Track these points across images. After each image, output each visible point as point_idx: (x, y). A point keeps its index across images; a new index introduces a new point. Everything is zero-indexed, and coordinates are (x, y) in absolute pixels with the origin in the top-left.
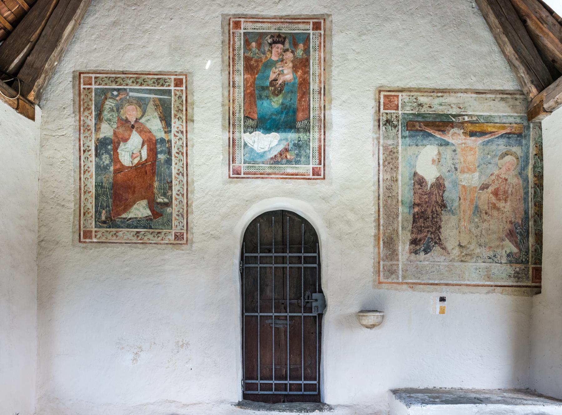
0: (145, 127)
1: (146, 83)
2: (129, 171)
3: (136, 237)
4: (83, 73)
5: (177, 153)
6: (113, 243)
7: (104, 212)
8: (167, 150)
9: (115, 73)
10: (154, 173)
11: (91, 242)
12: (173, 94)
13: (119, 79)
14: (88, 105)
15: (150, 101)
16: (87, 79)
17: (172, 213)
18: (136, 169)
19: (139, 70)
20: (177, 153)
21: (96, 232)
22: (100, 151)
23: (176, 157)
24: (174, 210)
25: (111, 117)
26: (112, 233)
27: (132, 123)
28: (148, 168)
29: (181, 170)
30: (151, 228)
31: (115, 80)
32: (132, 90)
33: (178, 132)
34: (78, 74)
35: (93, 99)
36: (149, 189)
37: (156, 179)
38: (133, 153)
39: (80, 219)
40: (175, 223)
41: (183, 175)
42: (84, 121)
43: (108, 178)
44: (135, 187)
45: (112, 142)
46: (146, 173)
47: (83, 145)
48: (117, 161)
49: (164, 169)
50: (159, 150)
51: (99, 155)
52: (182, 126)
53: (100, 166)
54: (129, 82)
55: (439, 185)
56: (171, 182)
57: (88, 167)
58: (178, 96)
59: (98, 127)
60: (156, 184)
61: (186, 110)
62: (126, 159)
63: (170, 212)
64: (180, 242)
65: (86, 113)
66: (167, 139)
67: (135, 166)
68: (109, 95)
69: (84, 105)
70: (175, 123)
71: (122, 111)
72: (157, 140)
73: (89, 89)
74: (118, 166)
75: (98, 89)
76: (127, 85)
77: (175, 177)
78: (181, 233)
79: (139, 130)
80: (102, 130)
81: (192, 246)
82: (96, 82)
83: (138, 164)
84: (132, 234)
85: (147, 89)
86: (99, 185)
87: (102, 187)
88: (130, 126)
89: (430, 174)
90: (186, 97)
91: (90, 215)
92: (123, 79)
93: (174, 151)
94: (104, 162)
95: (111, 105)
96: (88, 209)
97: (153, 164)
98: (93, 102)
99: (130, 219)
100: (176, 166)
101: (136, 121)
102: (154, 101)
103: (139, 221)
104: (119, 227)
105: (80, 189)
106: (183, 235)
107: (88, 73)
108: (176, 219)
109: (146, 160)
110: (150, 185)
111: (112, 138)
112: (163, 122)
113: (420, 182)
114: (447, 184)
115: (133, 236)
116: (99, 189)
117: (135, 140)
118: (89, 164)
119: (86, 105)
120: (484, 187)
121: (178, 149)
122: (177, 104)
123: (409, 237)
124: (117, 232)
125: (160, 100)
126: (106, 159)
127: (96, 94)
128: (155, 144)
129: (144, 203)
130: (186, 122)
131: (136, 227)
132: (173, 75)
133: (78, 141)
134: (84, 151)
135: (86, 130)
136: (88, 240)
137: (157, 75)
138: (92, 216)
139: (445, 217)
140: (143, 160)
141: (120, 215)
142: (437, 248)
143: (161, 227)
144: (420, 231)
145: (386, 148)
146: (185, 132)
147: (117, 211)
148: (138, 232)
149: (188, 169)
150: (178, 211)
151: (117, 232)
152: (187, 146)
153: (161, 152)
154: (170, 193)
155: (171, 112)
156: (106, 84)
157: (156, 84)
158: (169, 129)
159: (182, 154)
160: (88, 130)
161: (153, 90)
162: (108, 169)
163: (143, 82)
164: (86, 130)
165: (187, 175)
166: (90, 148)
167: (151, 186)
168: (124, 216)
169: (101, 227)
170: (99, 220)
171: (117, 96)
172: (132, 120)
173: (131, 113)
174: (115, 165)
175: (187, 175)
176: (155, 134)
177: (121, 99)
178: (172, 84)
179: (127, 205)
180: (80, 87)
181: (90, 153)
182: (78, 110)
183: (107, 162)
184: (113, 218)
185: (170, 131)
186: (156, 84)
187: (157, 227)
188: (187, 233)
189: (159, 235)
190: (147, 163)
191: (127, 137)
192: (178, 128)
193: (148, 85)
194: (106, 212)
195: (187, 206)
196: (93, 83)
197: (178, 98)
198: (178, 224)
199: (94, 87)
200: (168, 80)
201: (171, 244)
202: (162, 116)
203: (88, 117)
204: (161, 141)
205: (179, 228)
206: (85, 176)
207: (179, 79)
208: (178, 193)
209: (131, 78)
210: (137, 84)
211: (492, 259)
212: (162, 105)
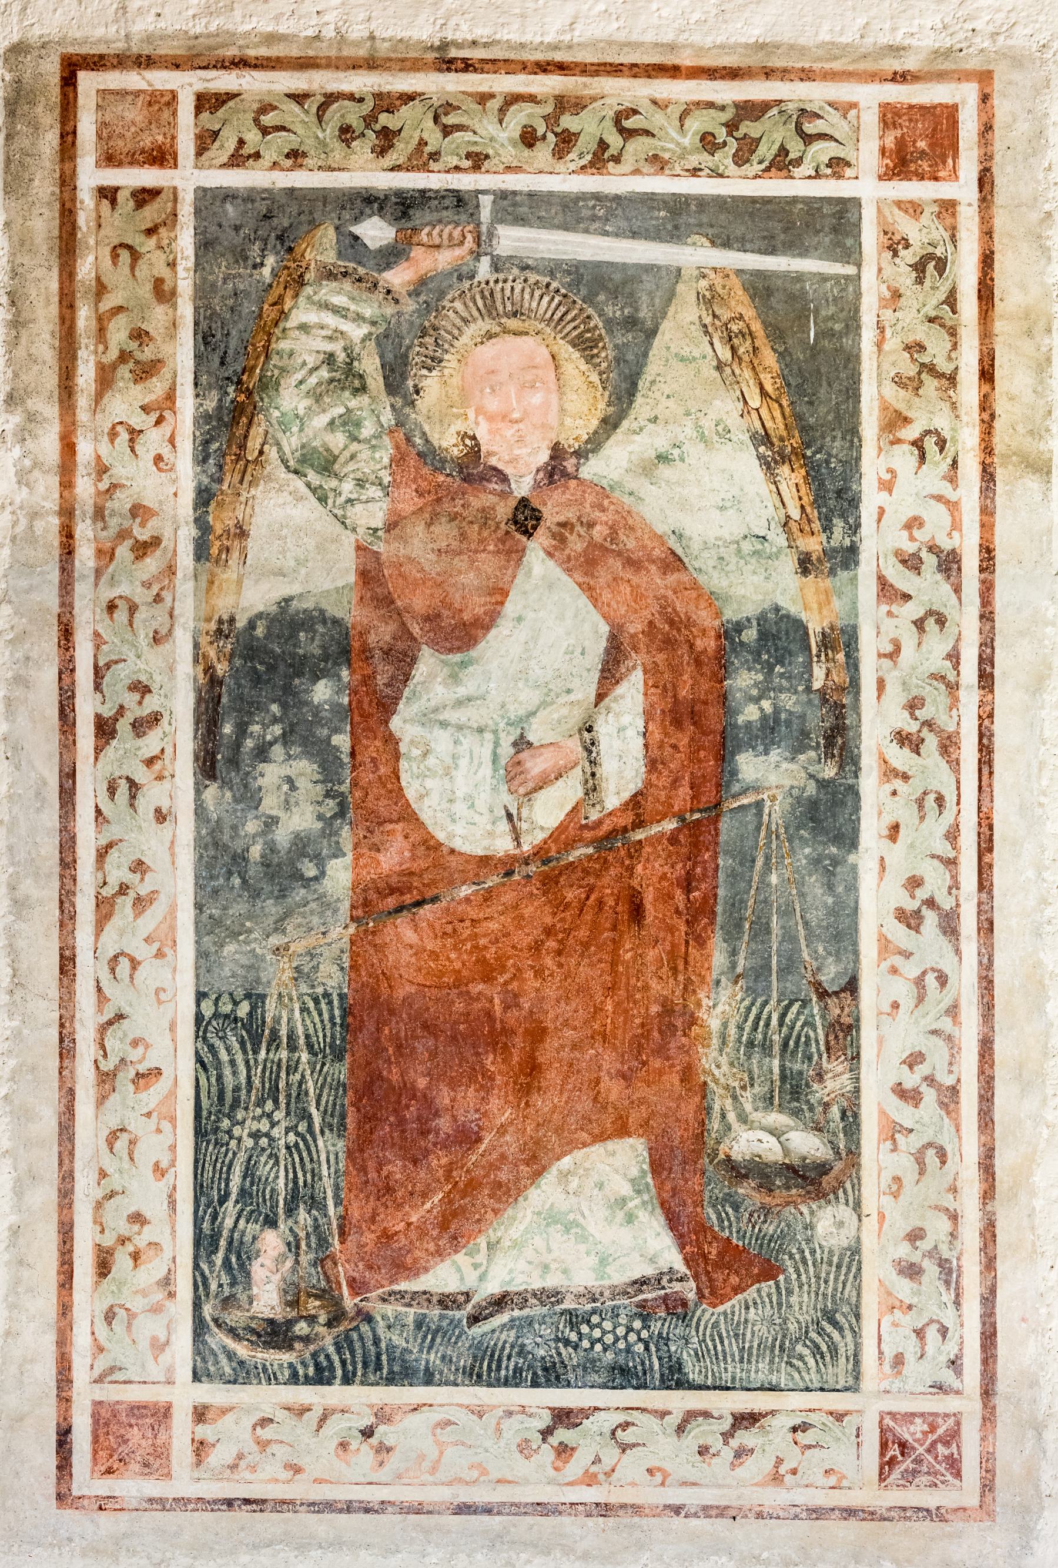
0: (624, 522)
1: (638, 147)
2: (488, 896)
3: (547, 1453)
4: (98, 63)
5: (902, 738)
6: (349, 1508)
7: (272, 1242)
8: (817, 720)
9: (371, 64)
10: (700, 914)
11: (159, 1503)
12: (870, 237)
13: (406, 113)
14: (139, 335)
15: (671, 296)
16: (134, 114)
17: (855, 1251)
18: (549, 882)
19: (581, 33)
20: (902, 738)
21: (200, 1414)
22: (242, 730)
23: (890, 773)
24: (873, 1224)
25: (338, 440)
26: (336, 1426)
27: (522, 488)
28: (652, 873)
29: (936, 881)
30: (675, 1378)
31: (377, 125)
32: (515, 208)
33: (911, 563)
34: (51, 70)
35: (185, 284)
36: (661, 1051)
37: (719, 959)
38: (522, 744)
39: (65, 1309)
40: (879, 1332)
41: (950, 927)
42: (102, 469)
43: (304, 959)
44: (538, 1034)
45: (343, 648)
46: (637, 912)
47: (98, 673)
48: (383, 808)
49: (786, 875)
50: (750, 714)
51: (234, 762)
52: (953, 506)
53: (240, 859)
54: (498, 135)
56: (852, 986)
57: (139, 867)
58: (909, 256)
59: (221, 520)
60: (720, 1008)
61: (987, 375)
62: (458, 790)
63: (840, 1240)
64: (930, 1499)
65: (125, 403)
66: (815, 627)
67: (541, 854)
68: (322, 248)
69: (101, 332)
70: (887, 486)
71: (432, 384)
72: (729, 634)
73: (144, 196)
74: (392, 858)
75: (228, 195)
76: (477, 161)
77: (885, 945)
78: (932, 1420)
79: (576, 545)
80: (258, 546)
81: (1026, 1532)
82: (205, 140)
83: (565, 835)
84: (513, 1427)
85: (649, 200)
86: (232, 1022)
87: (255, 1033)
88: (504, 511)
90: (987, 260)
91: (153, 1270)
92: (441, 112)
93: (876, 723)
94: (272, 822)
95: (337, 335)
96: (138, 1218)
97: (697, 837)
98: (186, 310)
99: (500, 1302)
100: (896, 854)
101: (557, 469)
102: (709, 300)
103: (574, 1319)
104: (402, 1373)
105: (66, 1049)
106: (953, 1436)
107: (145, 62)
108: (893, 1305)
109: (635, 802)
110: (668, 1009)
111: (349, 610)
112: (790, 477)
115: (524, 1448)
116: (229, 1047)
117: (548, 628)
118: (147, 840)
119: (118, 334)
121: (913, 706)
122: (910, 321)
124: (383, 1415)
125: (760, 287)
126: (289, 795)
127: (205, 245)
128: (720, 666)
129: (619, 1164)
130: (988, 475)
131: (551, 1375)
132: (873, 77)
133: (49, 643)
134: (105, 730)
135: (123, 551)
136: (131, 1487)
137: (733, 74)
138: (167, 1282)
140: (612, 801)
141: (402, 1267)
143: (761, 1371)
146: (971, 563)
147: (387, 1236)
148: (563, 1417)
149: (999, 878)
150: (915, 1236)
151: (383, 1415)
152: (986, 679)
153: (768, 732)
154: (835, 1083)
155: (853, 393)
156: (295, 155)
157: (724, 159)
158: (839, 536)
159: (948, 745)
160: (143, 549)
161: (702, 203)
162: (308, 882)
163: (615, 140)
164: (123, 551)
165: (987, 928)
166: (152, 704)
167: (675, 1021)
168: (443, 1277)
169: (243, 1373)
170: (235, 1317)
171: (391, 256)
172: (522, 462)
173: (510, 398)
174: (369, 844)
175: (987, 928)
176: (714, 580)
177: (421, 285)
178: (868, 154)
179: (472, 1186)
180: (67, 182)
181: (151, 743)
182: (51, 380)
183: (301, 820)
184: (349, 1302)
185: (849, 556)
186: (724, 159)
187: (732, 1370)
188: (989, 1419)
189: (746, 1438)
190: (639, 823)
191: (477, 605)
192: (913, 524)
193: (658, 163)
194: (294, 1246)
195: (988, 1194)
196: (186, 145)
197: (919, 268)
198: (910, 1347)
199: (188, 178)
200: (832, 123)
201: (849, 1513)
202: (776, 426)
203: (135, 434)
204: (764, 635)
205: (919, 1373)
206: (110, 942)
207: (925, 110)
208: (911, 1080)
209: (513, 99)
210: (559, 153)
212: (776, 333)
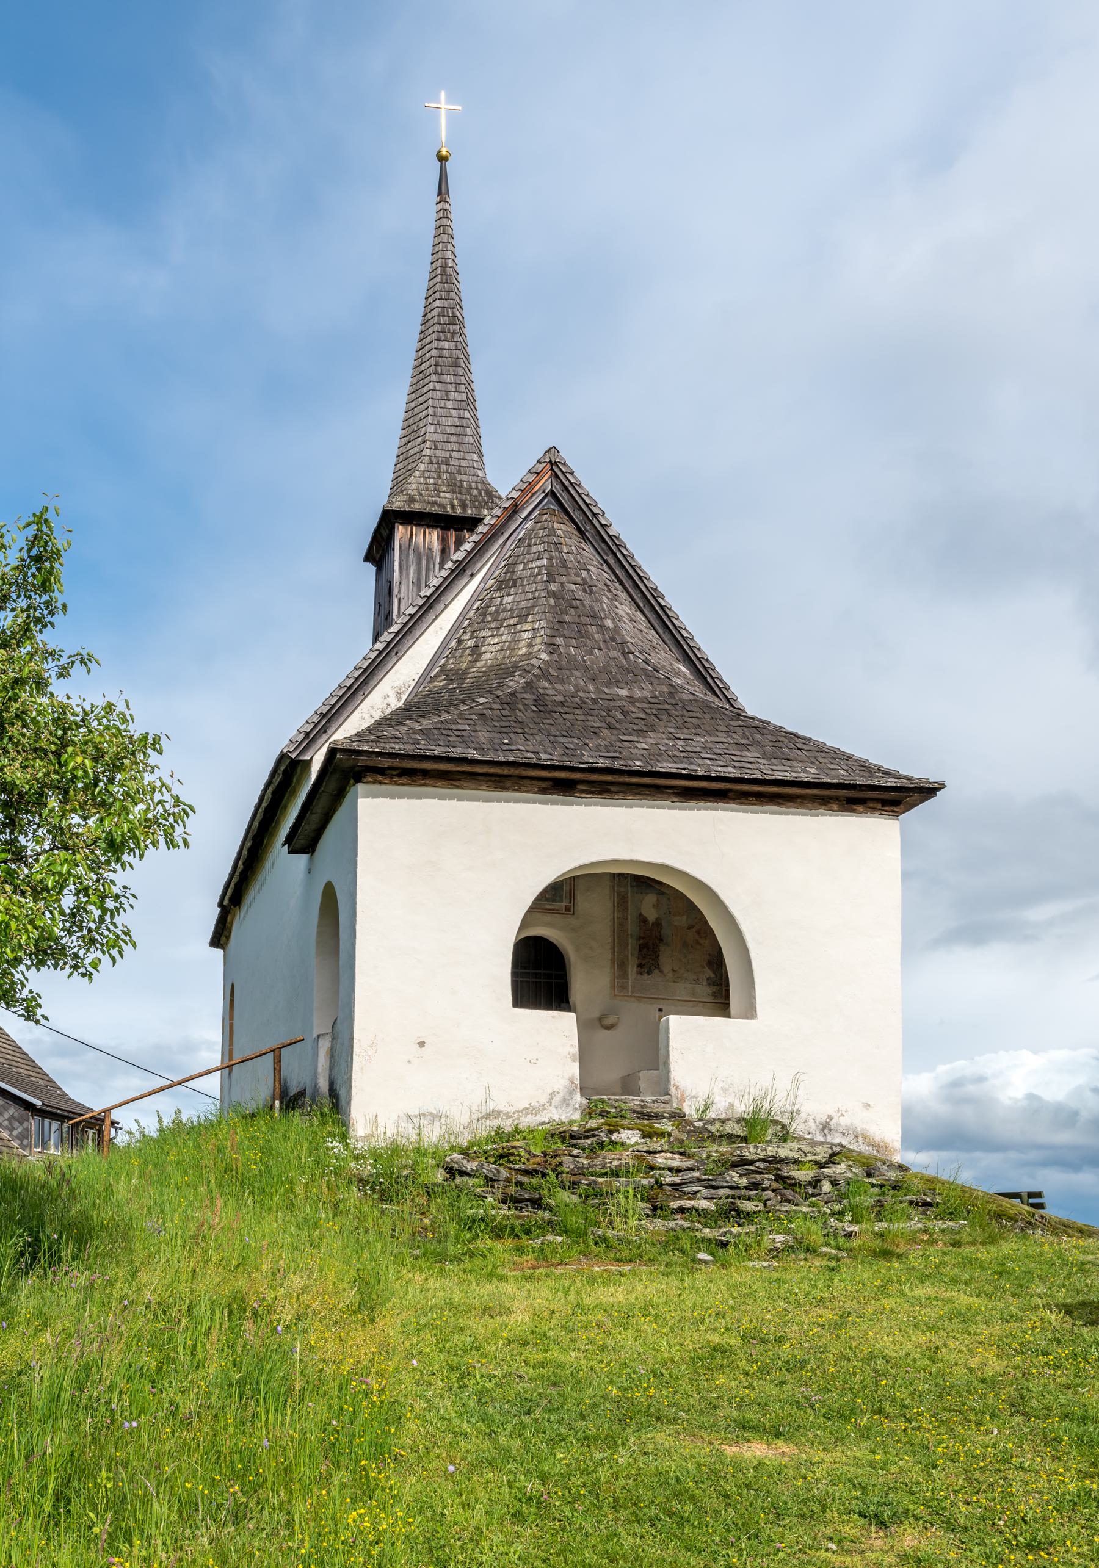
55: (658, 924)
89: (651, 915)
113: (644, 920)
114: (663, 923)
120: (690, 927)
123: (636, 961)
139: (662, 948)
142: (656, 971)
144: (644, 958)
145: (619, 894)
211: (696, 981)
